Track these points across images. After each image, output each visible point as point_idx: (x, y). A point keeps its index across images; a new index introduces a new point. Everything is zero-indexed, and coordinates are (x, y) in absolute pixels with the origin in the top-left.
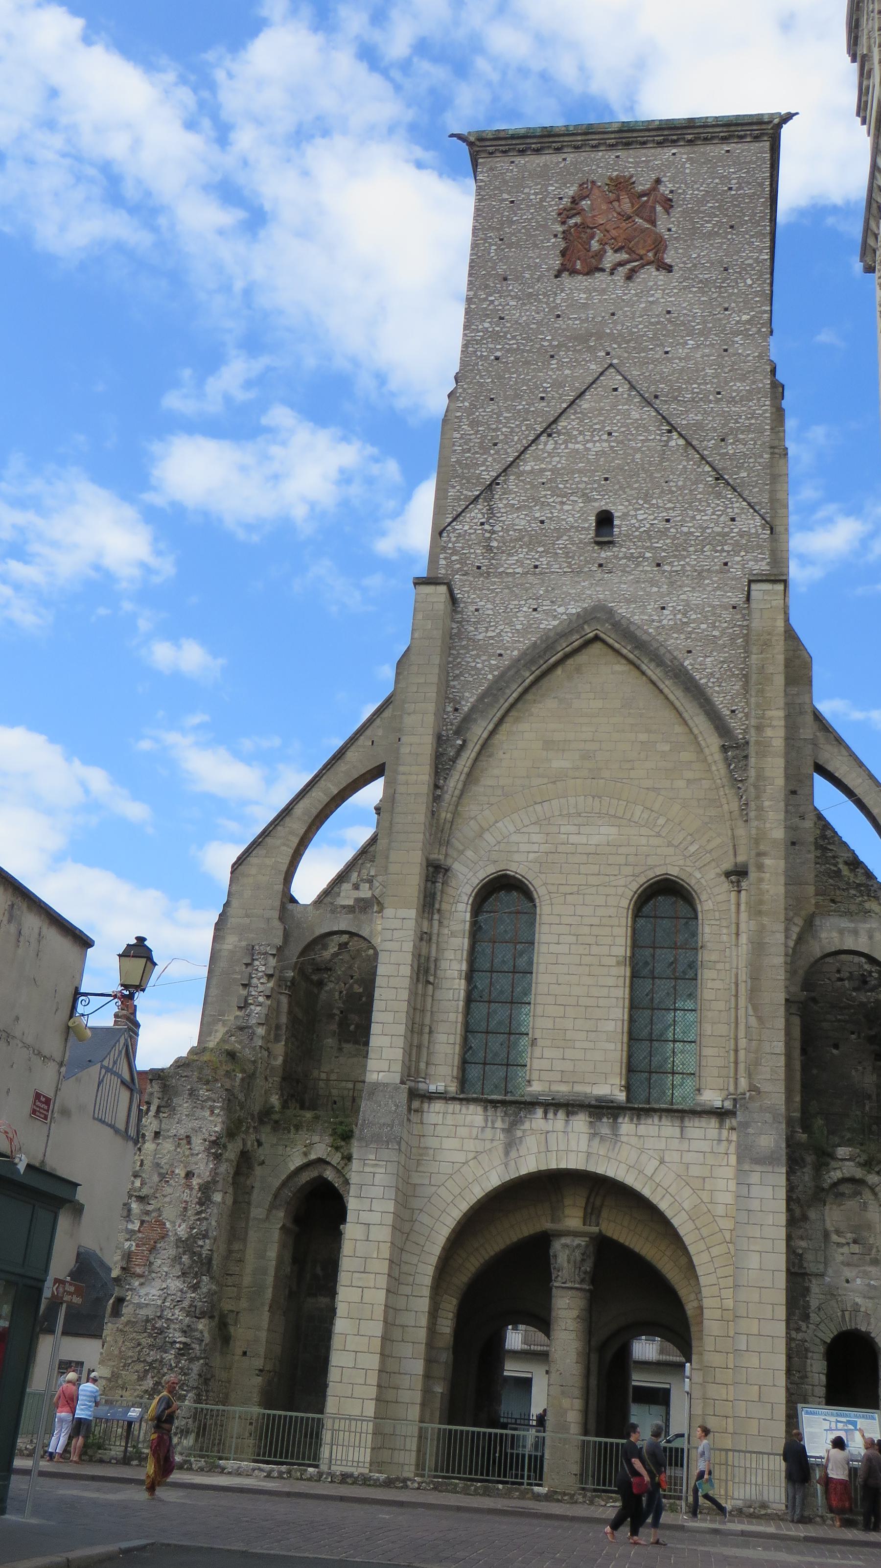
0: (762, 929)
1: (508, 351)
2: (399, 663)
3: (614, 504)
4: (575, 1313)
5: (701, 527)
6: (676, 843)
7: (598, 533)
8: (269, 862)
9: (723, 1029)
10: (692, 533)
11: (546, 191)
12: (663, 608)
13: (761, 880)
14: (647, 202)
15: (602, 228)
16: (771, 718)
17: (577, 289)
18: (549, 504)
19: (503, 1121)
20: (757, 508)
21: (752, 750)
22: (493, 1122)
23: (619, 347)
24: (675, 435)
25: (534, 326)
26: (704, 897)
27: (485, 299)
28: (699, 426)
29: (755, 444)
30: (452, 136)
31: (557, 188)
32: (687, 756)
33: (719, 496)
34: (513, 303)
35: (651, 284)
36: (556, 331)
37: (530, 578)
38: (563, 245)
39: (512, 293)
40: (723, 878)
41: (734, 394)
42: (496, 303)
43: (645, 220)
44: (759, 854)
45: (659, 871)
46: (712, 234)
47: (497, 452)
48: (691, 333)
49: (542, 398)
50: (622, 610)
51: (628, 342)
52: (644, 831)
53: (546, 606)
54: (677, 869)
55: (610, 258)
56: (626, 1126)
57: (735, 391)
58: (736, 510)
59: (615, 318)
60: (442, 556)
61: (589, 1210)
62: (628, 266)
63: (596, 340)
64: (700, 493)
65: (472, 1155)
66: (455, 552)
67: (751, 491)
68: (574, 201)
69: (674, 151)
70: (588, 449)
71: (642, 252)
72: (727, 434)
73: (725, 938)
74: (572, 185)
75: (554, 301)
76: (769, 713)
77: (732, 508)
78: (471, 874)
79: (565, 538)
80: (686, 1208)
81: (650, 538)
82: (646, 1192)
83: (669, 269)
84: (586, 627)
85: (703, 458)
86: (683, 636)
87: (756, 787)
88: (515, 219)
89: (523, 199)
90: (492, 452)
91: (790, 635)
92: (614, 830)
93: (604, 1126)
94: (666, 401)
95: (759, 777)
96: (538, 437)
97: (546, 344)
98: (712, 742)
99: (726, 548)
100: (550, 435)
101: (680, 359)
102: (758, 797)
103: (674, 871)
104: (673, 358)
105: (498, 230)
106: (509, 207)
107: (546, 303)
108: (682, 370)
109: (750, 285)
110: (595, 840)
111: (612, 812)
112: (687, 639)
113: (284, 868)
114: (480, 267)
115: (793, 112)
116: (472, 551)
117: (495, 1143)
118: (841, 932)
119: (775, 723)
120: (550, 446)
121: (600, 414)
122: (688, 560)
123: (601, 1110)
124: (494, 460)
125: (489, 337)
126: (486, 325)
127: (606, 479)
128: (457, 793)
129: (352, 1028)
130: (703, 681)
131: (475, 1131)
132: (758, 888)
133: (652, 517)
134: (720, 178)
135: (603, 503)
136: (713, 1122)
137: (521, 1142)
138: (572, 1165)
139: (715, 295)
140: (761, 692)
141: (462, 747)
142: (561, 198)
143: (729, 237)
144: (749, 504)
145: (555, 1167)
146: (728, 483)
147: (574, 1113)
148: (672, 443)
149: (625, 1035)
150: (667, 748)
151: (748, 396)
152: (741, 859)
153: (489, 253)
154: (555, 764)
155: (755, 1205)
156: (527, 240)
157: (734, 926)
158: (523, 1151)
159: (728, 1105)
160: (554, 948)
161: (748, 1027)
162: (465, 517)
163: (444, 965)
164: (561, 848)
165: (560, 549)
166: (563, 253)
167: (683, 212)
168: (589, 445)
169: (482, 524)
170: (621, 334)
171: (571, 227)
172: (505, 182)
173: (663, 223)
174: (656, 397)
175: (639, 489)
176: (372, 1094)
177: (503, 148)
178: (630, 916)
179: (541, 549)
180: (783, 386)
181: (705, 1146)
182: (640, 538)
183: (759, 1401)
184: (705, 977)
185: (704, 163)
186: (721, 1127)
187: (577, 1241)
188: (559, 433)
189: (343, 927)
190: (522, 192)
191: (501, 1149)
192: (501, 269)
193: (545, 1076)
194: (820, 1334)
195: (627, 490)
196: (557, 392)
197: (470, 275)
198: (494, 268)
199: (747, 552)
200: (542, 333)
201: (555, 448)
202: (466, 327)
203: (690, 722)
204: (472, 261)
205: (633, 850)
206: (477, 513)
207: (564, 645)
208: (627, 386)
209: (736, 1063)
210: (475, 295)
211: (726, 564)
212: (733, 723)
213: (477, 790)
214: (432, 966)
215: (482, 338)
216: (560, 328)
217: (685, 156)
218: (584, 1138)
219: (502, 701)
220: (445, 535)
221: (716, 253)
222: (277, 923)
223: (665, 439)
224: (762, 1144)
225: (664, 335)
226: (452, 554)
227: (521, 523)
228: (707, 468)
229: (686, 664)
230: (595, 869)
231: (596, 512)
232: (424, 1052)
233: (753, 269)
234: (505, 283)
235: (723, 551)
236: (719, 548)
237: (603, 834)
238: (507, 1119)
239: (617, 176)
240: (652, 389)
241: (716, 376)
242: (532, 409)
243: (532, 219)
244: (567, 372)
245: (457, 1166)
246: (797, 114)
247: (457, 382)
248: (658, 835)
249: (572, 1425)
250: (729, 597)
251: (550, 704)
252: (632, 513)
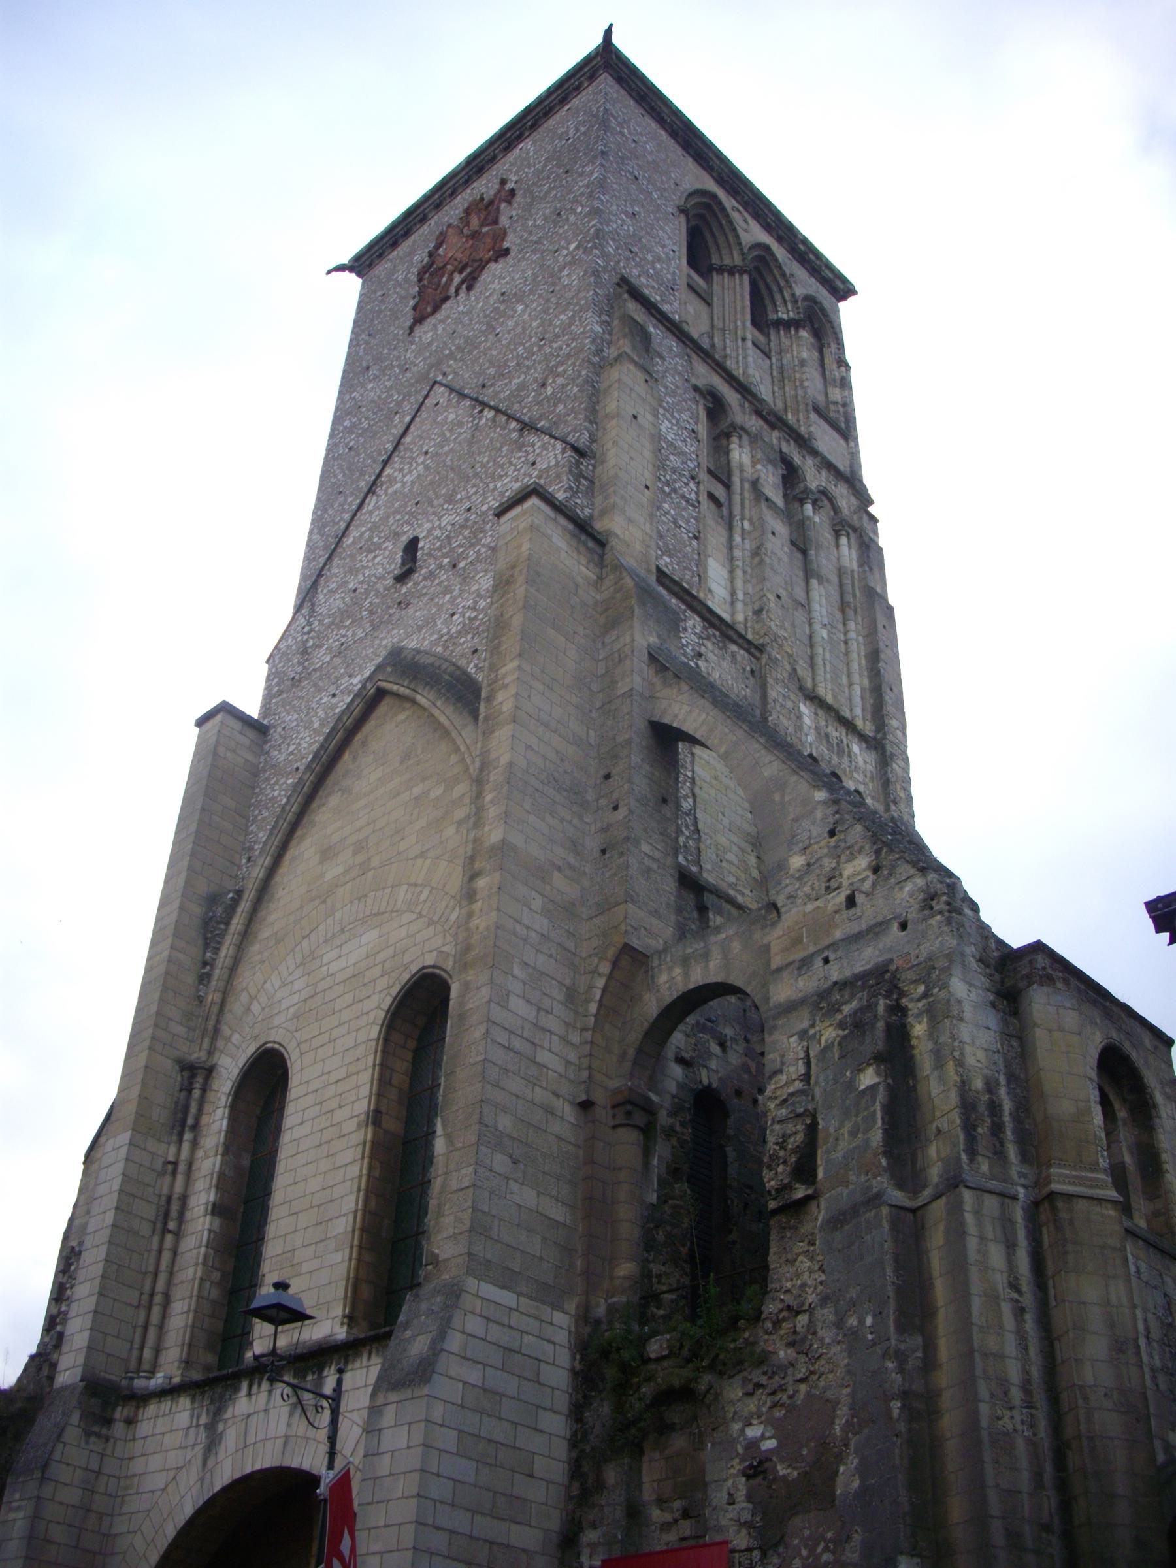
6: (436, 918)
12: (453, 615)
30: (329, 272)
45: (414, 968)
92: (374, 934)
118: (685, 961)
230: (348, 998)
232: (152, 1333)
238: (212, 1407)
246: (611, 25)
251: (334, 801)
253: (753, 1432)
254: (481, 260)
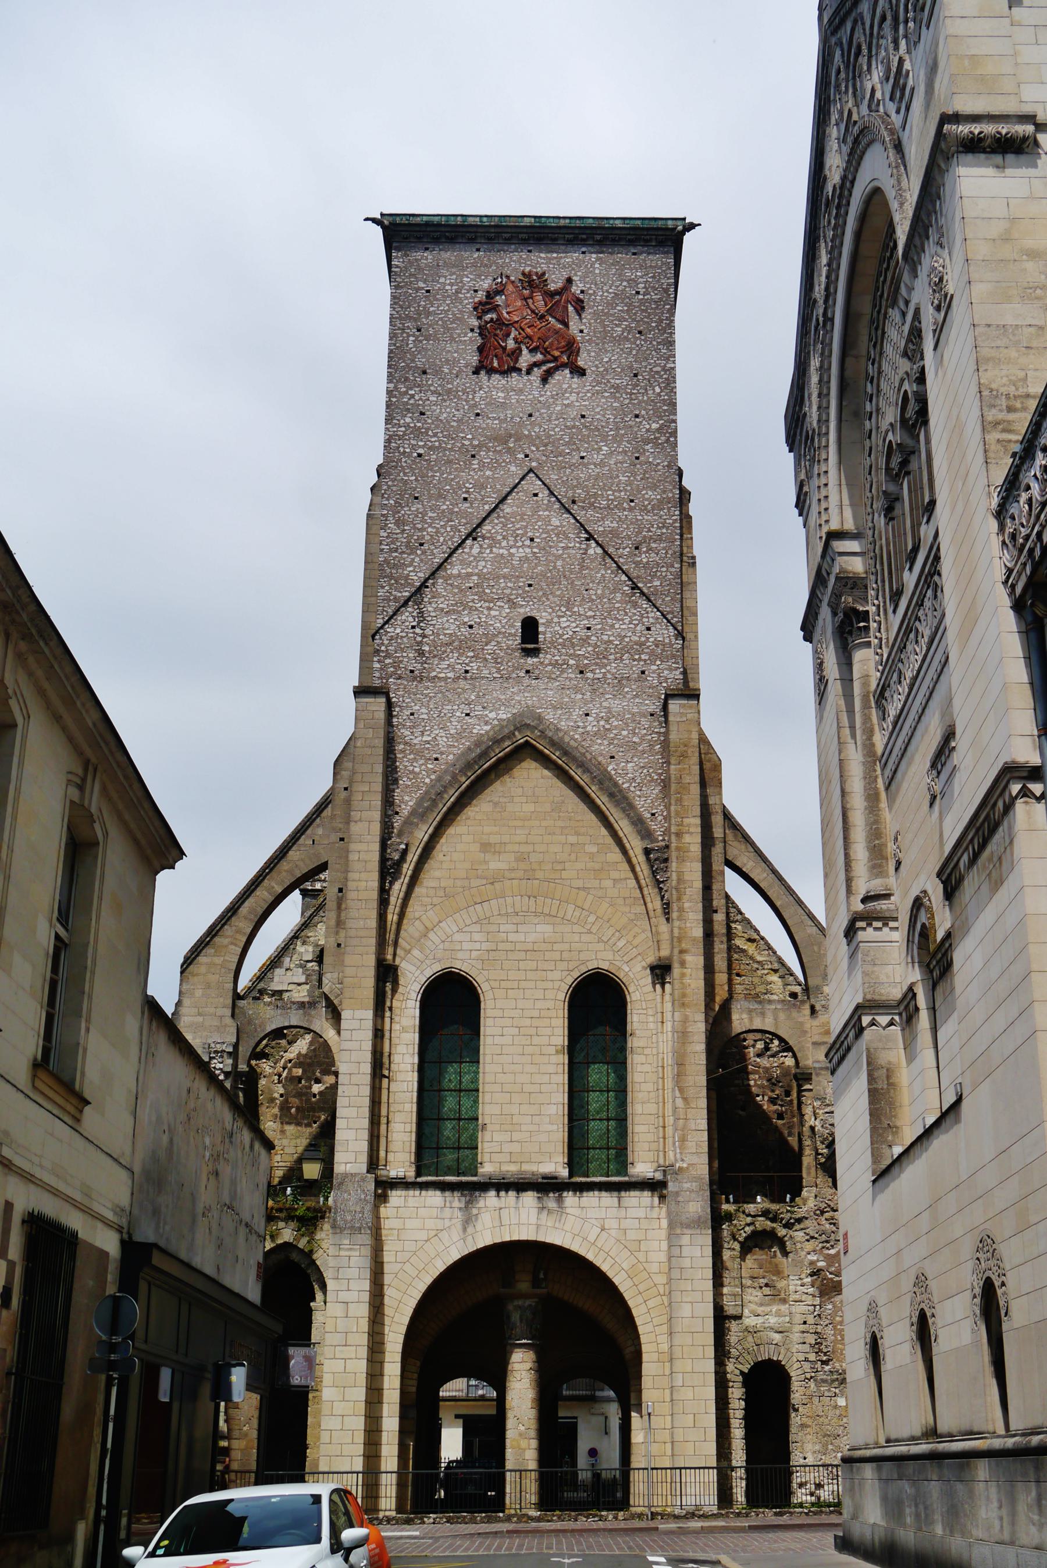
0: (685, 1020)
1: (430, 448)
2: (337, 763)
3: (539, 610)
4: (529, 1365)
5: (619, 635)
6: (605, 939)
7: (524, 641)
8: (218, 960)
9: (652, 1108)
10: (611, 642)
11: (461, 282)
12: (587, 715)
13: (683, 975)
14: (559, 301)
15: (516, 325)
16: (689, 825)
17: (494, 387)
18: (476, 609)
20: (669, 617)
21: (674, 855)
23: (537, 449)
24: (593, 544)
25: (455, 424)
26: (631, 989)
27: (406, 393)
28: (614, 533)
29: (667, 553)
30: (367, 219)
31: (472, 280)
32: (616, 855)
33: (635, 605)
34: (433, 398)
35: (565, 386)
36: (476, 430)
37: (462, 683)
38: (480, 341)
39: (432, 388)
40: (648, 971)
41: (646, 503)
42: (417, 397)
43: (558, 320)
44: (681, 952)
45: (591, 965)
46: (621, 340)
47: (424, 552)
48: (604, 438)
49: (465, 499)
50: (550, 716)
51: (546, 445)
52: (576, 928)
53: (478, 710)
54: (608, 963)
55: (526, 358)
56: (570, 1199)
57: (647, 500)
58: (651, 620)
59: (533, 419)
60: (375, 659)
62: (544, 368)
63: (516, 441)
64: (617, 602)
65: (434, 1233)
66: (388, 655)
67: (663, 600)
68: (490, 295)
69: (584, 249)
70: (512, 555)
71: (557, 353)
72: (641, 543)
73: (652, 1026)
74: (486, 277)
75: (473, 399)
76: (686, 821)
77: (648, 617)
78: (419, 971)
79: (493, 643)
81: (573, 645)
82: (590, 1257)
83: (581, 372)
84: (517, 733)
85: (619, 568)
86: (606, 742)
87: (677, 889)
88: (431, 309)
89: (439, 289)
90: (419, 552)
91: (703, 740)
92: (549, 928)
93: (551, 1201)
94: (583, 507)
95: (680, 880)
96: (464, 541)
97: (467, 443)
98: (636, 845)
99: (643, 657)
100: (475, 539)
101: (595, 465)
102: (679, 899)
103: (605, 966)
104: (589, 464)
105: (415, 320)
106: (426, 297)
107: (466, 401)
108: (597, 478)
109: (659, 394)
110: (531, 938)
111: (546, 911)
112: (610, 744)
113: (234, 967)
114: (400, 359)
115: (696, 222)
116: (405, 654)
117: (454, 1221)
119: (692, 830)
120: (476, 550)
121: (522, 519)
122: (608, 668)
123: (547, 1186)
124: (421, 560)
125: (411, 433)
126: (408, 420)
127: (530, 585)
128: (402, 895)
129: (293, 1110)
130: (625, 786)
132: (682, 983)
133: (574, 625)
134: (628, 281)
135: (528, 610)
136: (647, 1194)
137: (476, 1220)
138: (523, 1237)
139: (627, 401)
140: (679, 801)
141: (405, 852)
142: (476, 291)
143: (638, 342)
144: (663, 615)
145: (508, 1239)
146: (643, 593)
147: (525, 1190)
148: (591, 552)
149: (566, 1117)
150: (594, 849)
151: (660, 505)
152: (665, 953)
153: (408, 345)
154: (493, 865)
155: (687, 1263)
156: (444, 333)
157: (660, 1015)
159: (659, 1176)
160: (498, 1040)
161: (675, 1109)
162: (396, 620)
163: (396, 1058)
164: (501, 946)
165: (490, 654)
166: (481, 350)
167: (594, 313)
168: (513, 551)
169: (413, 627)
170: (538, 437)
171: (487, 323)
172: (420, 269)
173: (574, 326)
174: (574, 502)
175: (561, 597)
176: (341, 1184)
177: (418, 234)
178: (566, 1008)
179: (471, 654)
180: (690, 494)
181: (641, 1213)
182: (563, 645)
184: (635, 1062)
185: (612, 264)
186: (652, 1196)
187: (528, 1302)
188: (484, 538)
189: (294, 1023)
190: (438, 281)
191: (459, 1226)
192: (420, 362)
193: (496, 1157)
194: (740, 1366)
195: (550, 597)
196: (479, 493)
197: (389, 366)
198: (413, 361)
199: (662, 661)
200: (463, 431)
201: (480, 553)
202: (388, 421)
203: (616, 826)
204: (391, 352)
205: (566, 946)
206: (407, 616)
207: (497, 751)
208: (547, 492)
209: (664, 1138)
210: (396, 387)
211: (643, 672)
212: (653, 826)
213: (418, 890)
214: (386, 1060)
215: (405, 434)
216: (479, 427)
217: (594, 256)
218: (534, 1212)
219: (441, 806)
220: (377, 637)
221: (626, 358)
222: (229, 1020)
223: (584, 546)
224: (691, 1210)
225: (580, 440)
226: (385, 657)
227: (451, 629)
228: (624, 578)
229: (609, 769)
230: (533, 965)
231: (521, 618)
233: (661, 377)
234: (424, 376)
235: (640, 659)
236: (637, 657)
237: (540, 931)
239: (530, 271)
240: (570, 494)
241: (629, 483)
242: (456, 510)
243: (448, 310)
244: (488, 473)
245: (420, 1244)
247: (379, 475)
248: (590, 932)
250: (647, 705)
252: (556, 620)
253: (813, 1257)
254: (556, 359)
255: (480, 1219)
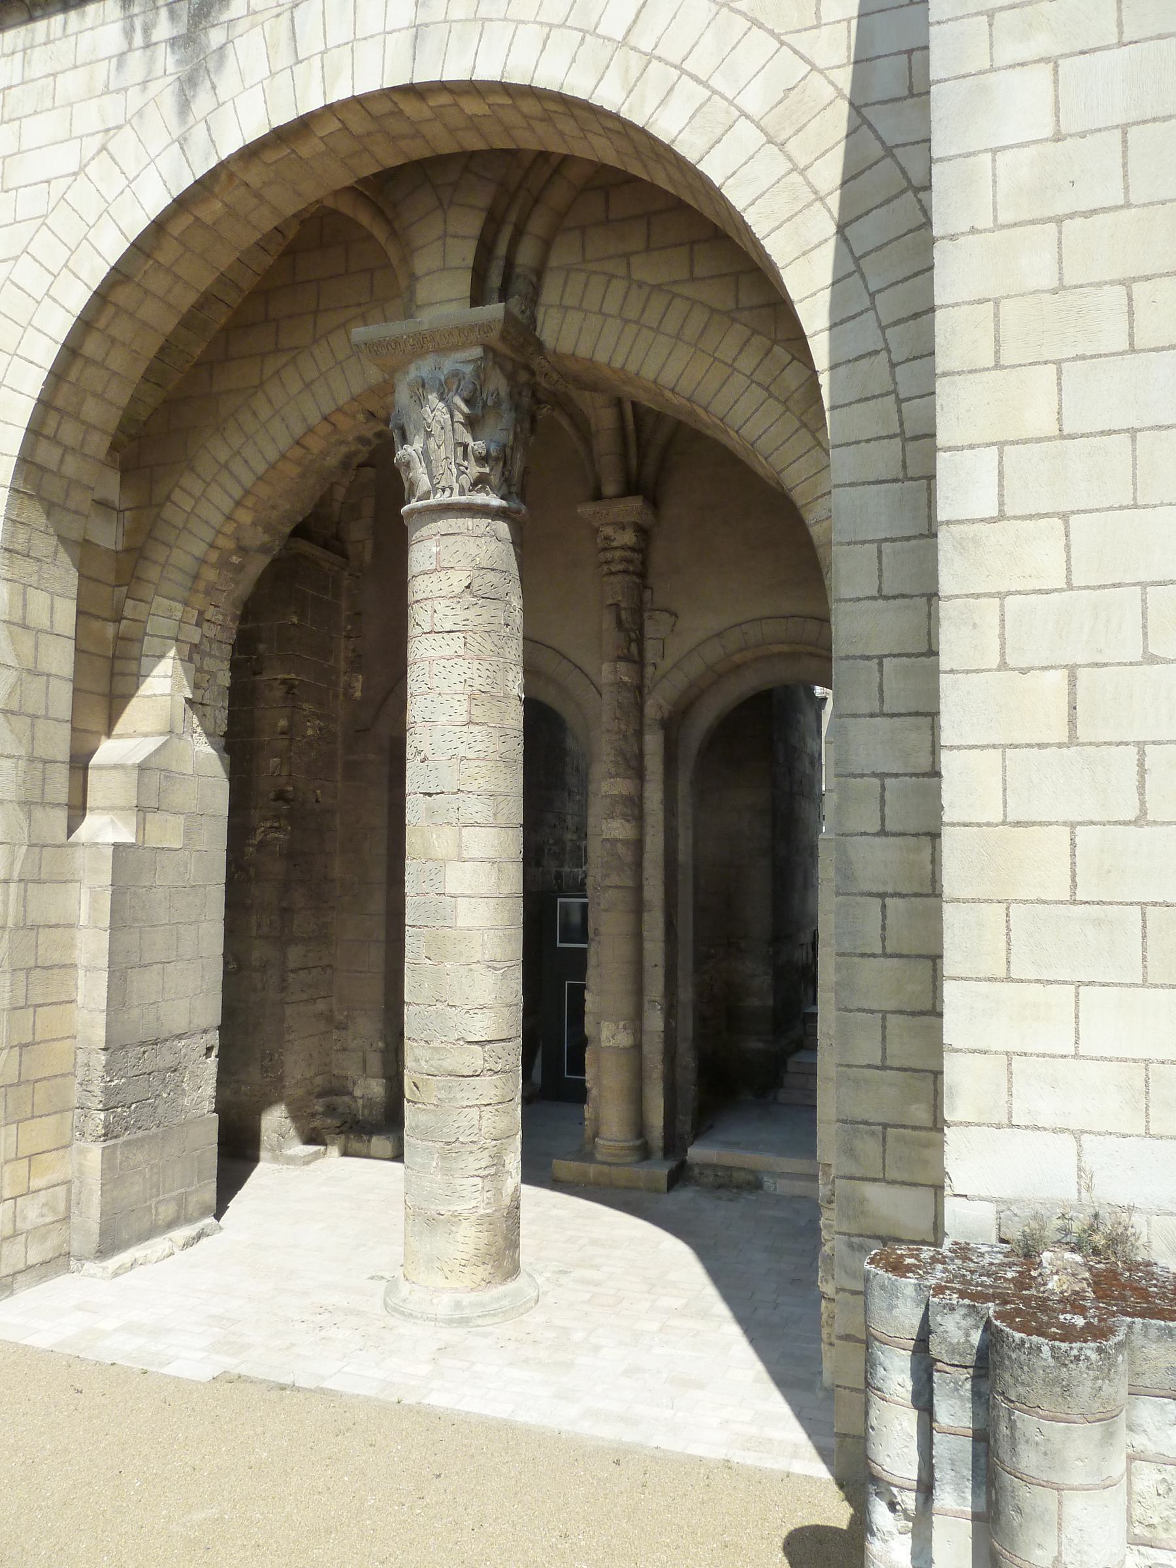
19: (173, 16)
22: (147, 30)
61: (495, 280)
65: (94, 143)
80: (749, 110)
131: (101, 70)
158: (227, 83)
183: (1073, 740)
187: (450, 363)
191: (169, 102)
249: (462, 904)
255: (230, 62)
